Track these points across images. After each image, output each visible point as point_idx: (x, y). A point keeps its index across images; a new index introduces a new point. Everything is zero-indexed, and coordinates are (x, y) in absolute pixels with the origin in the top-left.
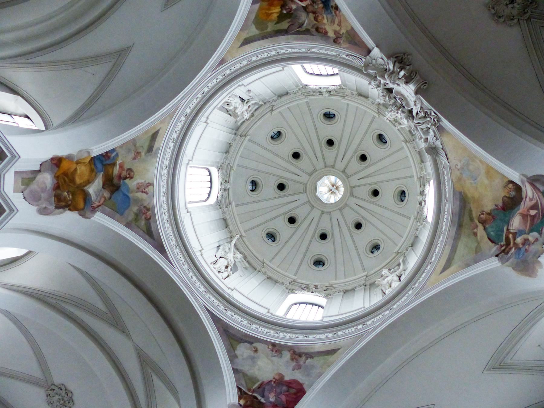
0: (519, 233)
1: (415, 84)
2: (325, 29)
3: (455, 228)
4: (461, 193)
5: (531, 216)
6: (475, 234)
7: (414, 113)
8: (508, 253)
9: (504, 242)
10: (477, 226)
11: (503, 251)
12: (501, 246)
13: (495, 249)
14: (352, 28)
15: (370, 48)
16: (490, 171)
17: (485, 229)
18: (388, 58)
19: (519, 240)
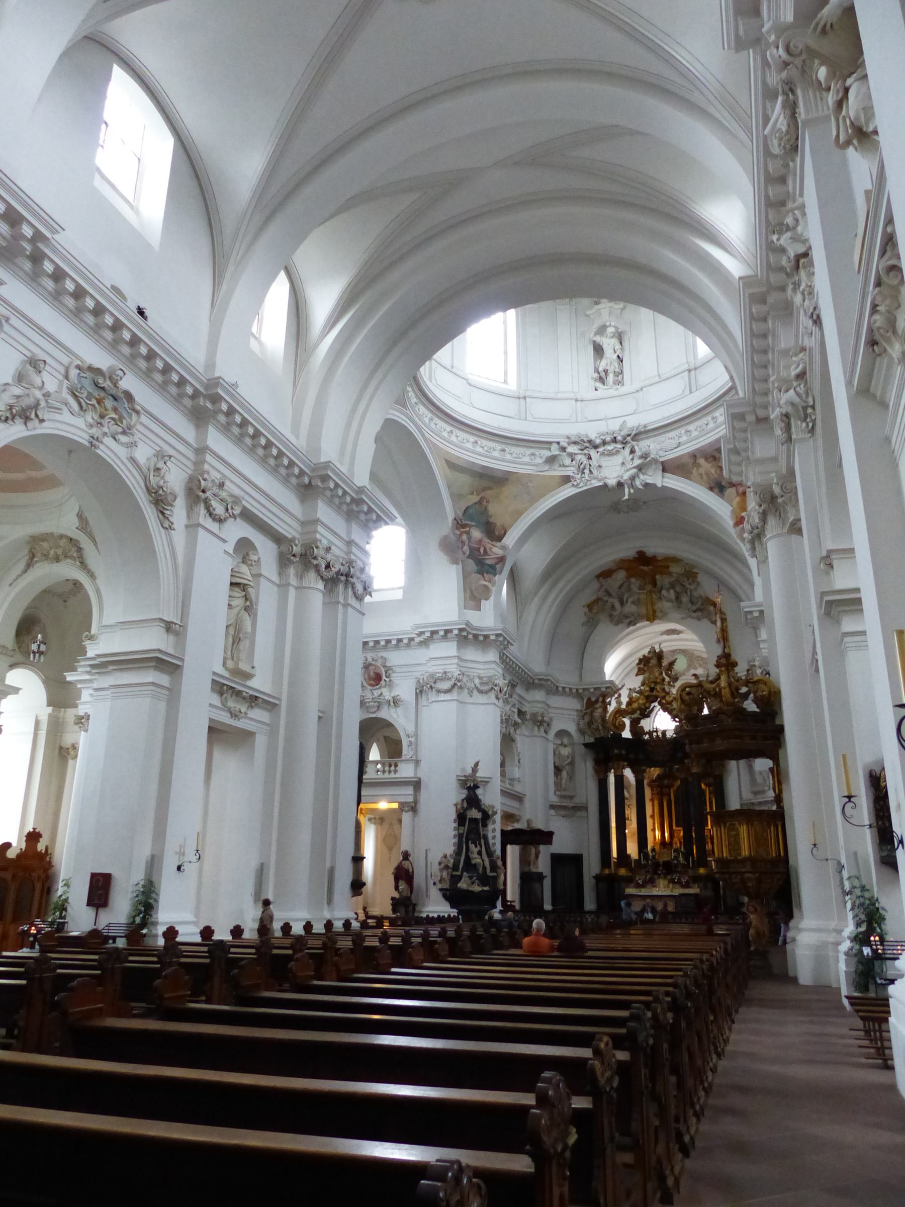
0: (469, 538)
1: (613, 486)
2: (709, 463)
3: (480, 471)
4: (507, 480)
5: (479, 548)
6: (472, 494)
7: (593, 453)
8: (457, 528)
9: (464, 522)
10: (478, 495)
11: (458, 523)
12: (461, 520)
13: (460, 514)
14: (690, 479)
15: (666, 474)
16: (517, 515)
17: (476, 503)
18: (646, 485)
19: (465, 537)
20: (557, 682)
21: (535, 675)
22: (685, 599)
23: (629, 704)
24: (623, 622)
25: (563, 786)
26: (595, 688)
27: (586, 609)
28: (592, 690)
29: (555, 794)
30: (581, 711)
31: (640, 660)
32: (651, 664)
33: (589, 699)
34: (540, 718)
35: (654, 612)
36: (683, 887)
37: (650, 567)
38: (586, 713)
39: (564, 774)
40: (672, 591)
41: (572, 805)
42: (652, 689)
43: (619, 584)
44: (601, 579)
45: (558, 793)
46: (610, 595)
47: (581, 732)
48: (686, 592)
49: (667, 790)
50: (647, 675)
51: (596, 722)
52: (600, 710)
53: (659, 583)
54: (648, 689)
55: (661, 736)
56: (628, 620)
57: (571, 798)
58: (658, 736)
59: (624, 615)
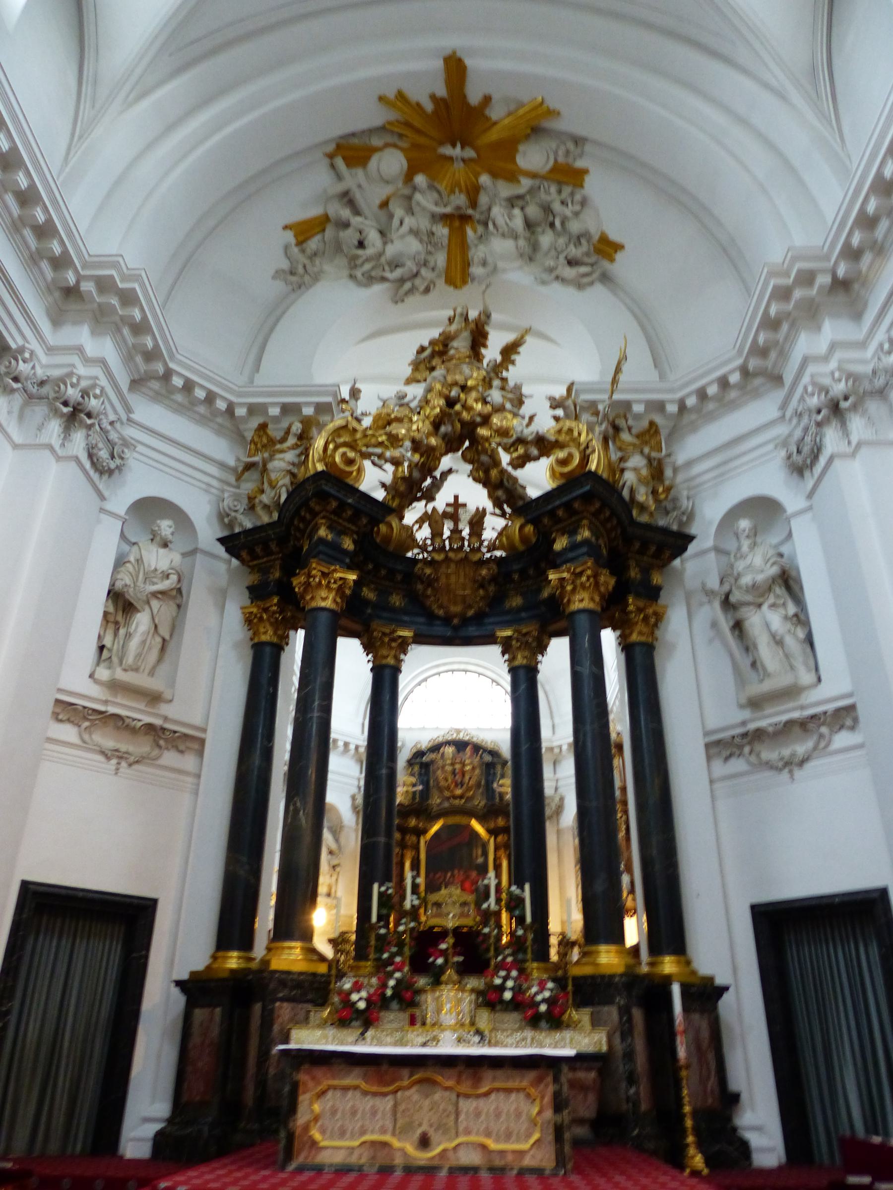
20: (172, 357)
21: (85, 266)
22: (546, 239)
23: (384, 421)
24: (383, 279)
25: (130, 659)
26: (287, 409)
27: (290, 237)
28: (275, 411)
29: (91, 676)
30: (234, 470)
31: (422, 349)
32: (452, 352)
33: (263, 427)
34: (72, 393)
35: (466, 264)
36: (534, 1021)
37: (470, 153)
38: (249, 467)
39: (141, 621)
40: (517, 212)
41: (147, 719)
42: (451, 403)
43: (384, 191)
44: (340, 162)
45: (103, 674)
46: (357, 212)
47: (223, 517)
48: (552, 225)
49: (414, 838)
50: (439, 372)
51: (273, 486)
52: (290, 456)
53: (483, 199)
54: (442, 402)
55: (466, 533)
56: (398, 273)
57: (154, 698)
58: (456, 531)
59: (389, 264)
